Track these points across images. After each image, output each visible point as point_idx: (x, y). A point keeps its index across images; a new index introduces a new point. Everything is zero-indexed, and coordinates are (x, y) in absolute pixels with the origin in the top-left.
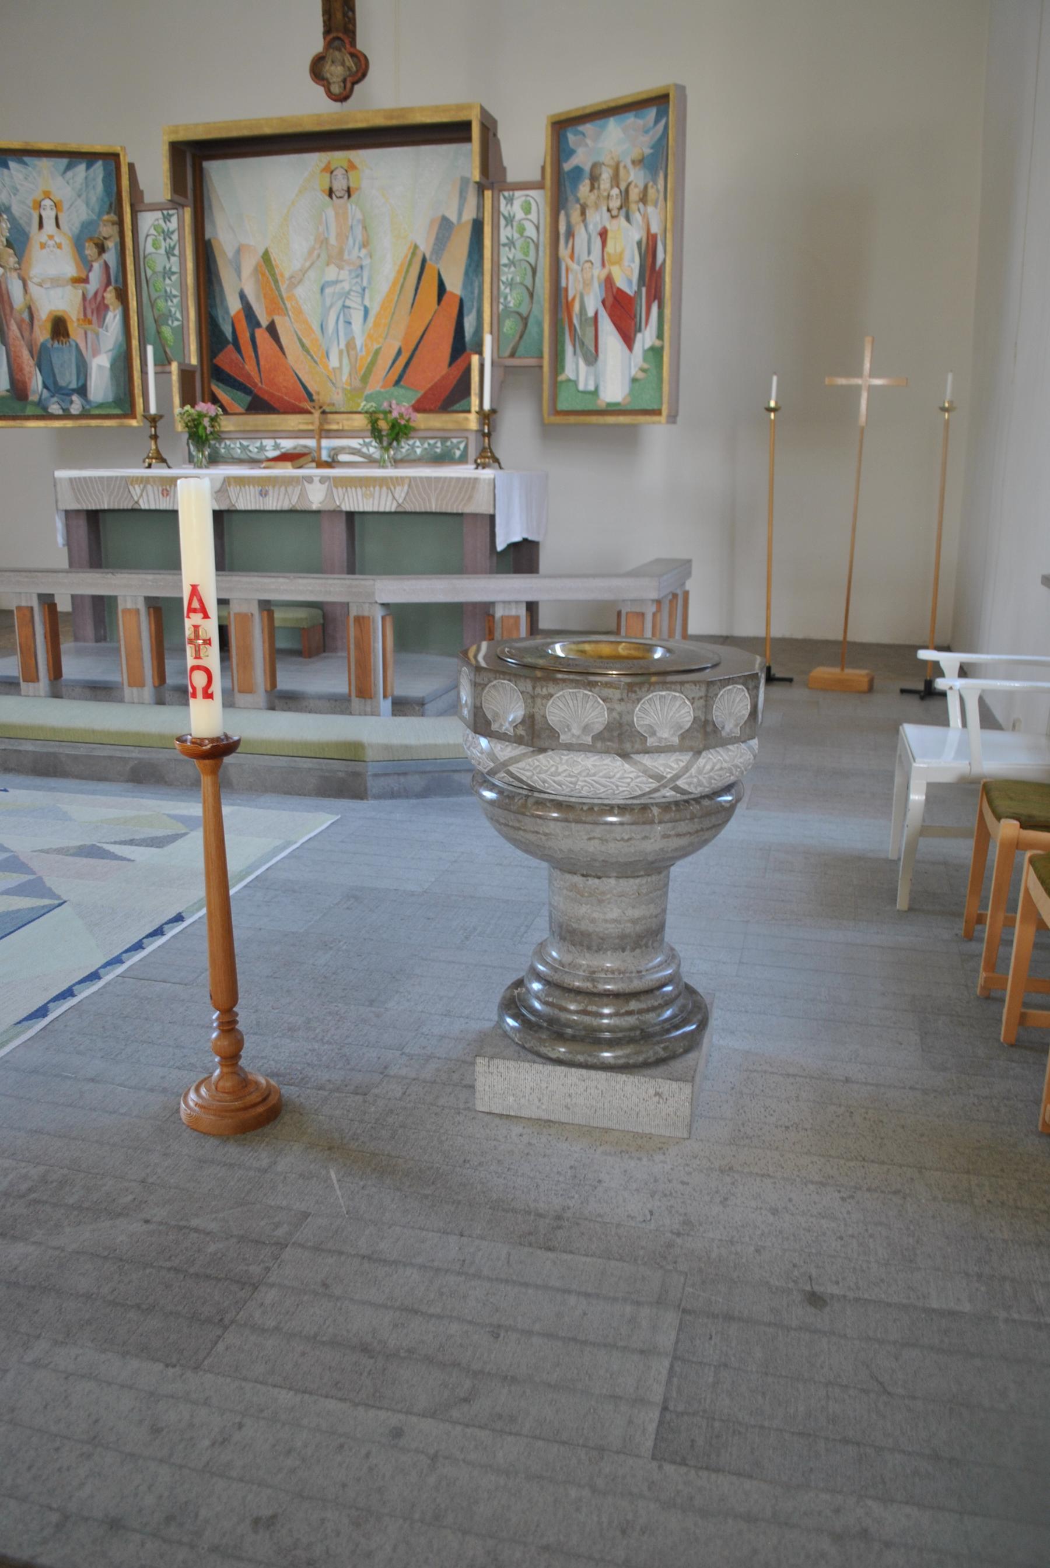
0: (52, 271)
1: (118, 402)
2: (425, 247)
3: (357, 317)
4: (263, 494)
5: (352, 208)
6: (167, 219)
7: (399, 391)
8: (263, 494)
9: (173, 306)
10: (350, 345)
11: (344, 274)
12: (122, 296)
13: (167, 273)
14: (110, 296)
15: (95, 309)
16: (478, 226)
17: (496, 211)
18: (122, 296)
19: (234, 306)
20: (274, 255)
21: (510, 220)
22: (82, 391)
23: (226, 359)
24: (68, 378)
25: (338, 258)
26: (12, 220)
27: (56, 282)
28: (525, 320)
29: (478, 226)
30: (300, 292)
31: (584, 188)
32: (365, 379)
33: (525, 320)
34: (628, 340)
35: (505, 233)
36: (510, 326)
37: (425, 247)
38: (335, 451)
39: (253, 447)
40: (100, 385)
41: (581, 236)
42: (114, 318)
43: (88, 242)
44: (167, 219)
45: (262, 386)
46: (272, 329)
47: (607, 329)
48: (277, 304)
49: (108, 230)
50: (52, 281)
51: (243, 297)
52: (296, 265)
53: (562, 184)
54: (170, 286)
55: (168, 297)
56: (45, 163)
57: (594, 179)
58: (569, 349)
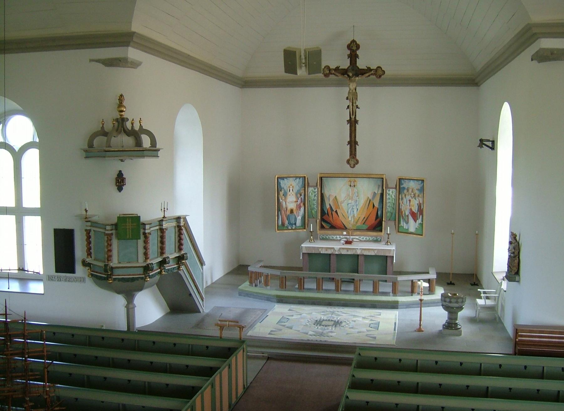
0: (291, 200)
1: (302, 226)
2: (370, 198)
3: (355, 211)
4: (348, 251)
5: (355, 189)
6: (315, 189)
7: (364, 226)
8: (348, 251)
9: (315, 206)
10: (354, 216)
11: (353, 202)
12: (304, 205)
13: (314, 200)
14: (302, 204)
15: (299, 207)
16: (382, 195)
17: (386, 192)
18: (304, 205)
19: (328, 207)
20: (337, 197)
21: (389, 194)
22: (295, 224)
23: (325, 217)
24: (293, 221)
25: (352, 199)
26: (284, 190)
27: (292, 202)
28: (392, 214)
29: (382, 195)
30: (343, 205)
31: (405, 191)
32: (357, 223)
33: (392, 214)
34: (415, 221)
35: (388, 197)
36: (388, 214)
37: (370, 198)
38: (353, 239)
39: (335, 237)
40: (299, 222)
41: (405, 200)
42: (302, 209)
43: (298, 194)
44: (315, 189)
45: (333, 223)
46: (336, 212)
47: (410, 217)
48: (338, 206)
49: (303, 191)
50: (291, 202)
51: (330, 205)
52: (342, 199)
53: (400, 189)
54: (315, 202)
55: (314, 205)
56: (291, 179)
57: (408, 190)
58: (402, 220)
